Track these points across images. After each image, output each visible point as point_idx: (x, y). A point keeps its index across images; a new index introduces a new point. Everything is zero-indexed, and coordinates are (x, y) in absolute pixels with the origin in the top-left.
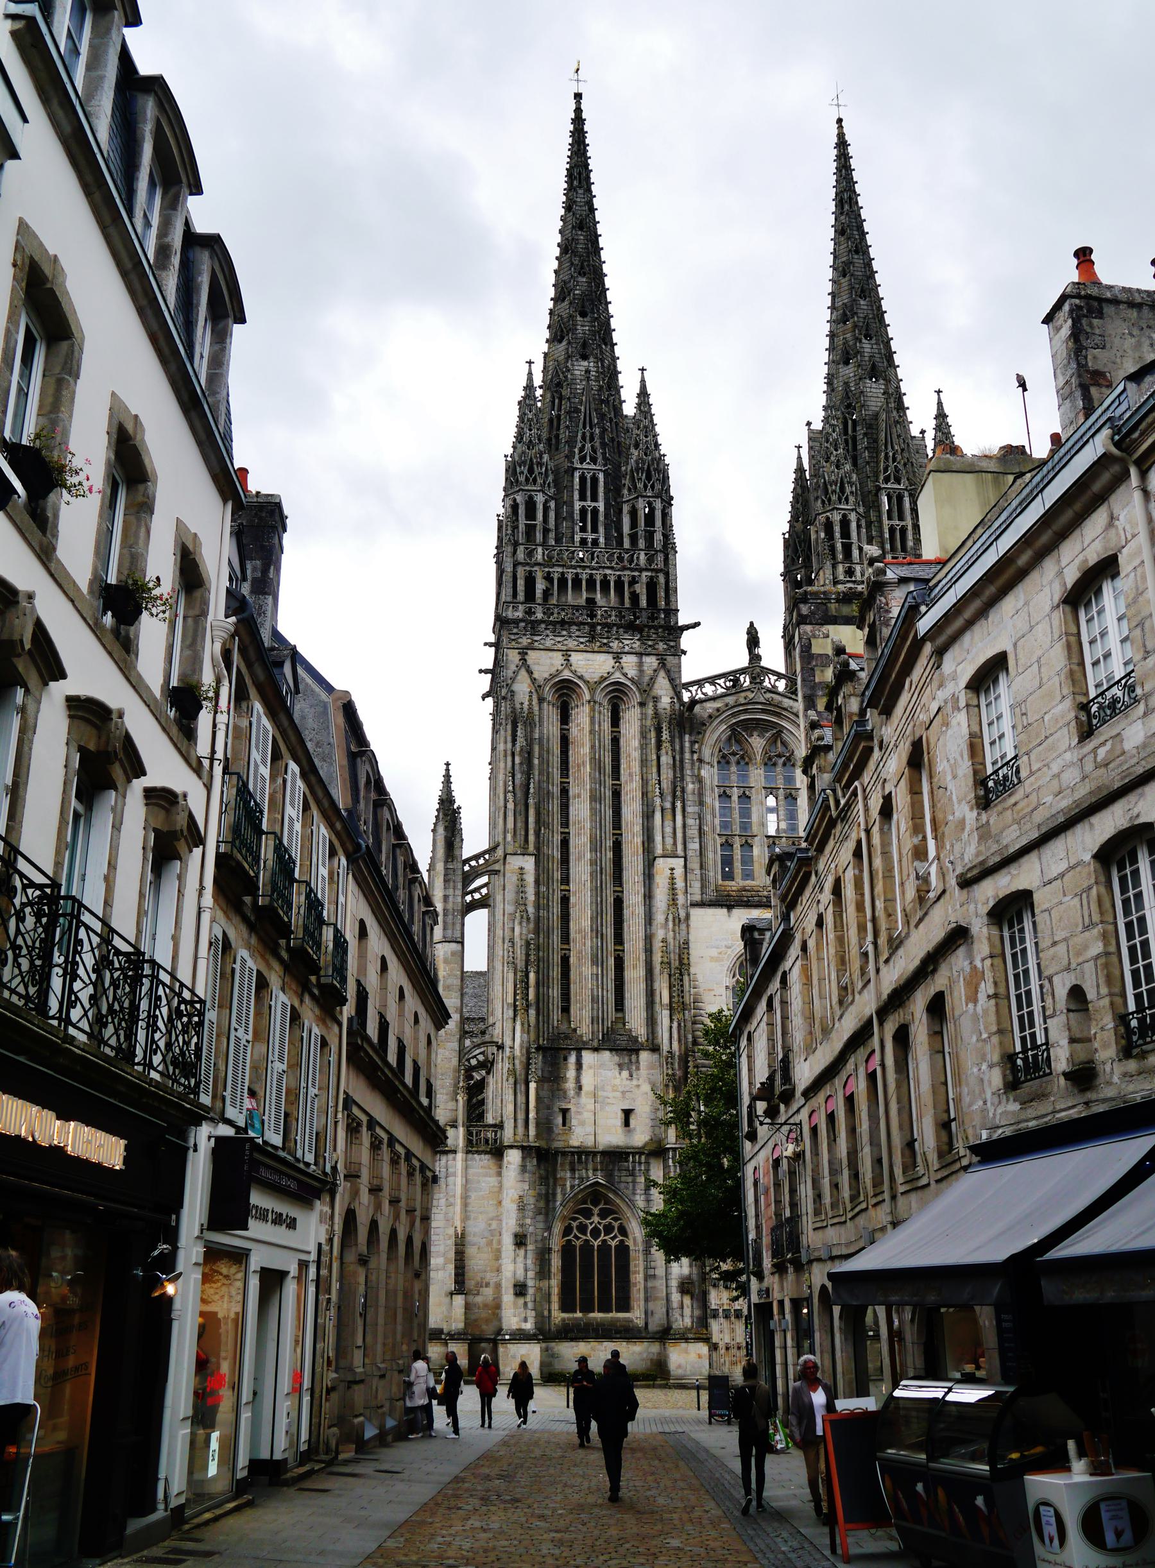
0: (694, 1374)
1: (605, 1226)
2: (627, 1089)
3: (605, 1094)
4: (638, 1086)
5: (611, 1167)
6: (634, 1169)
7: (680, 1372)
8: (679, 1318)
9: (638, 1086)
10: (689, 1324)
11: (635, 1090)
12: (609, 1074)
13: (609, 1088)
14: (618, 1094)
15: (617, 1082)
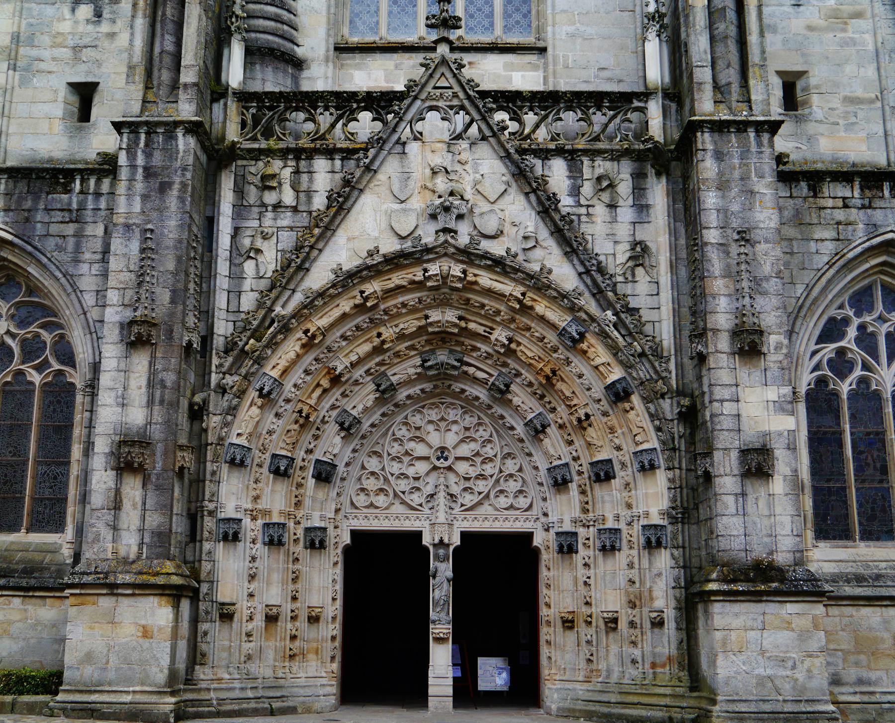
0: (129, 681)
1: (24, 342)
2: (87, 41)
3: (34, 53)
4: (112, 35)
5: (28, 204)
6: (81, 208)
7: (89, 672)
8: (107, 534)
9: (112, 35)
10: (134, 549)
11: (106, 43)
12: (50, 10)
13: (46, 40)
14: (66, 53)
15: (66, 27)
